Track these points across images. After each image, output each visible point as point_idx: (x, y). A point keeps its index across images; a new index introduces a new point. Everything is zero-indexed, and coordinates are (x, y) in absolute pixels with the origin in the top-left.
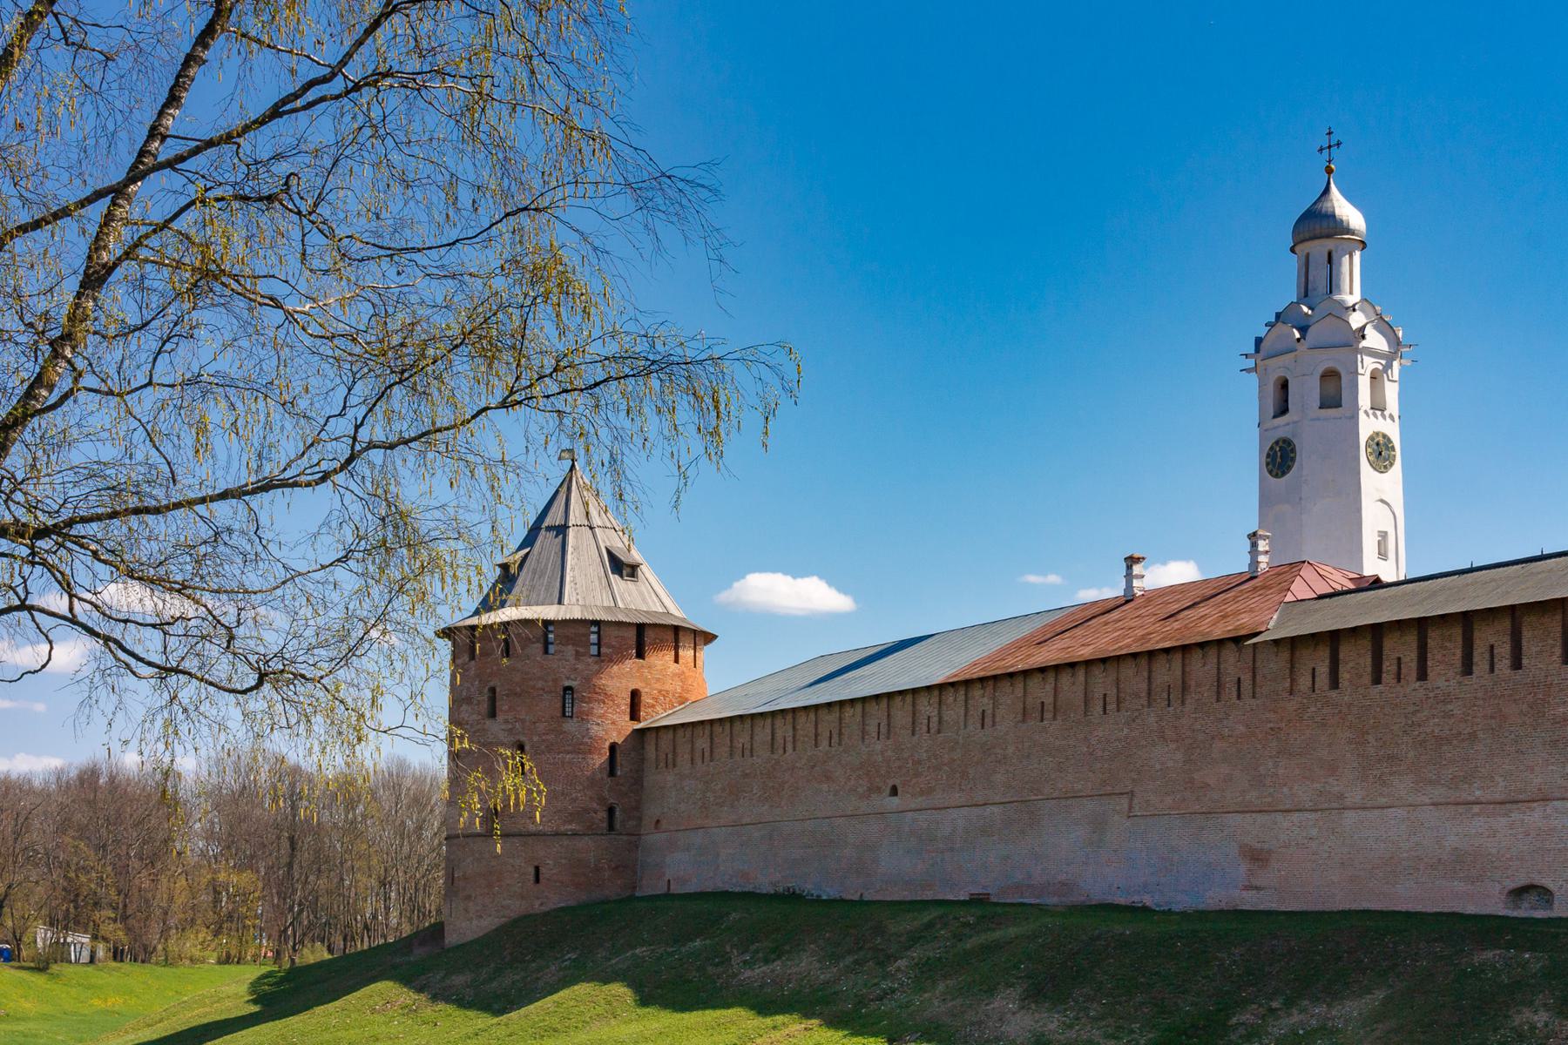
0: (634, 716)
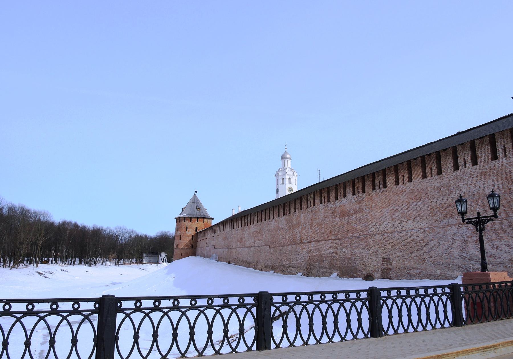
0: (196, 230)
